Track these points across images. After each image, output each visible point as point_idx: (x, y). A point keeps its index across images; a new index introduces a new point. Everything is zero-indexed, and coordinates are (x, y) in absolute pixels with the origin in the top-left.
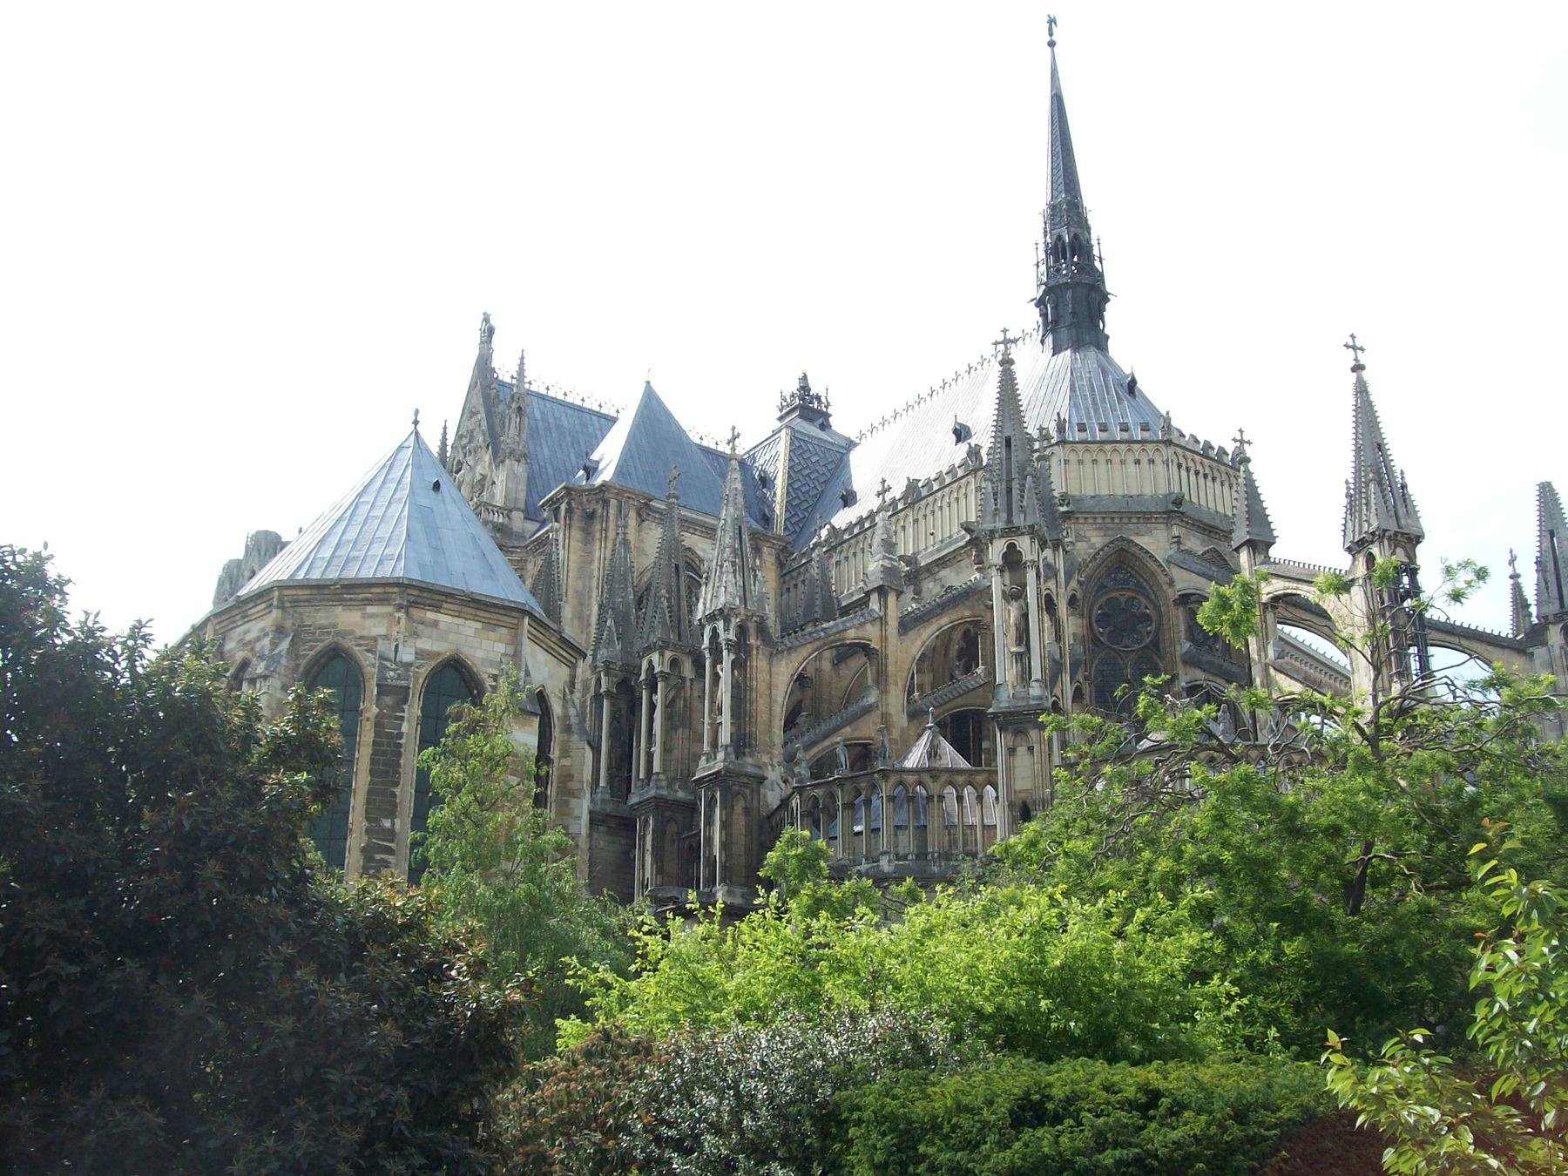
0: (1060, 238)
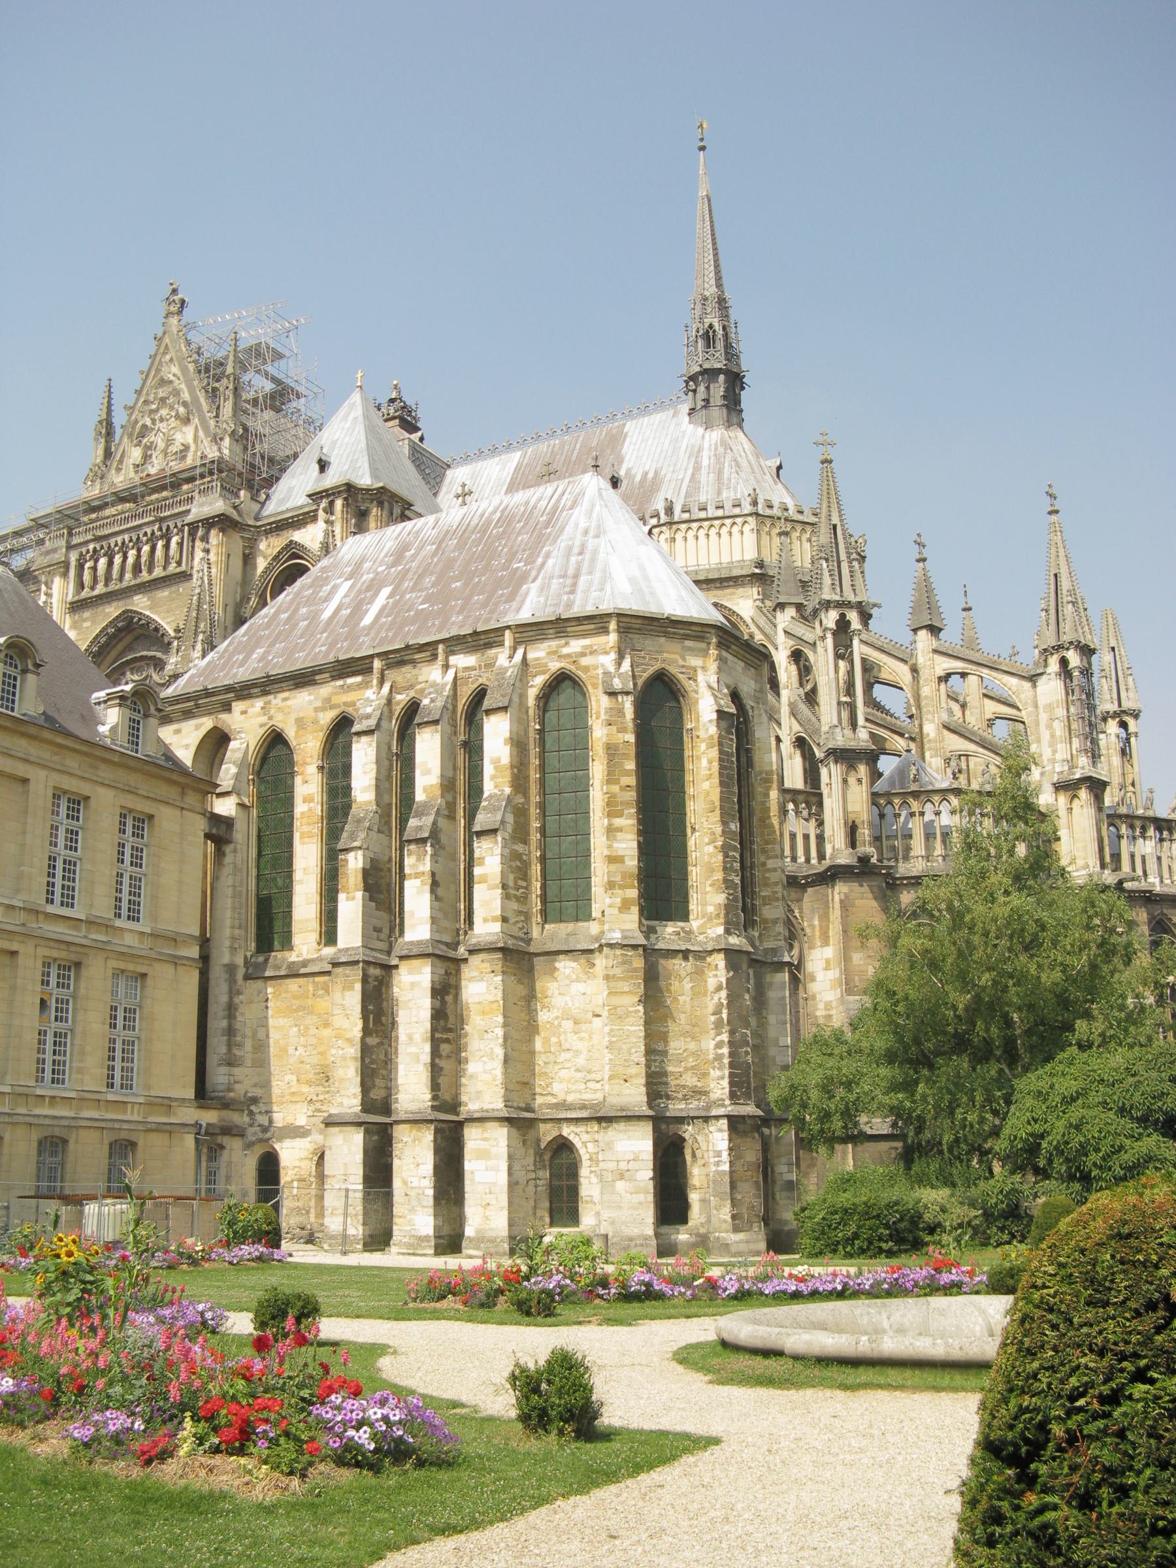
0: (711, 326)
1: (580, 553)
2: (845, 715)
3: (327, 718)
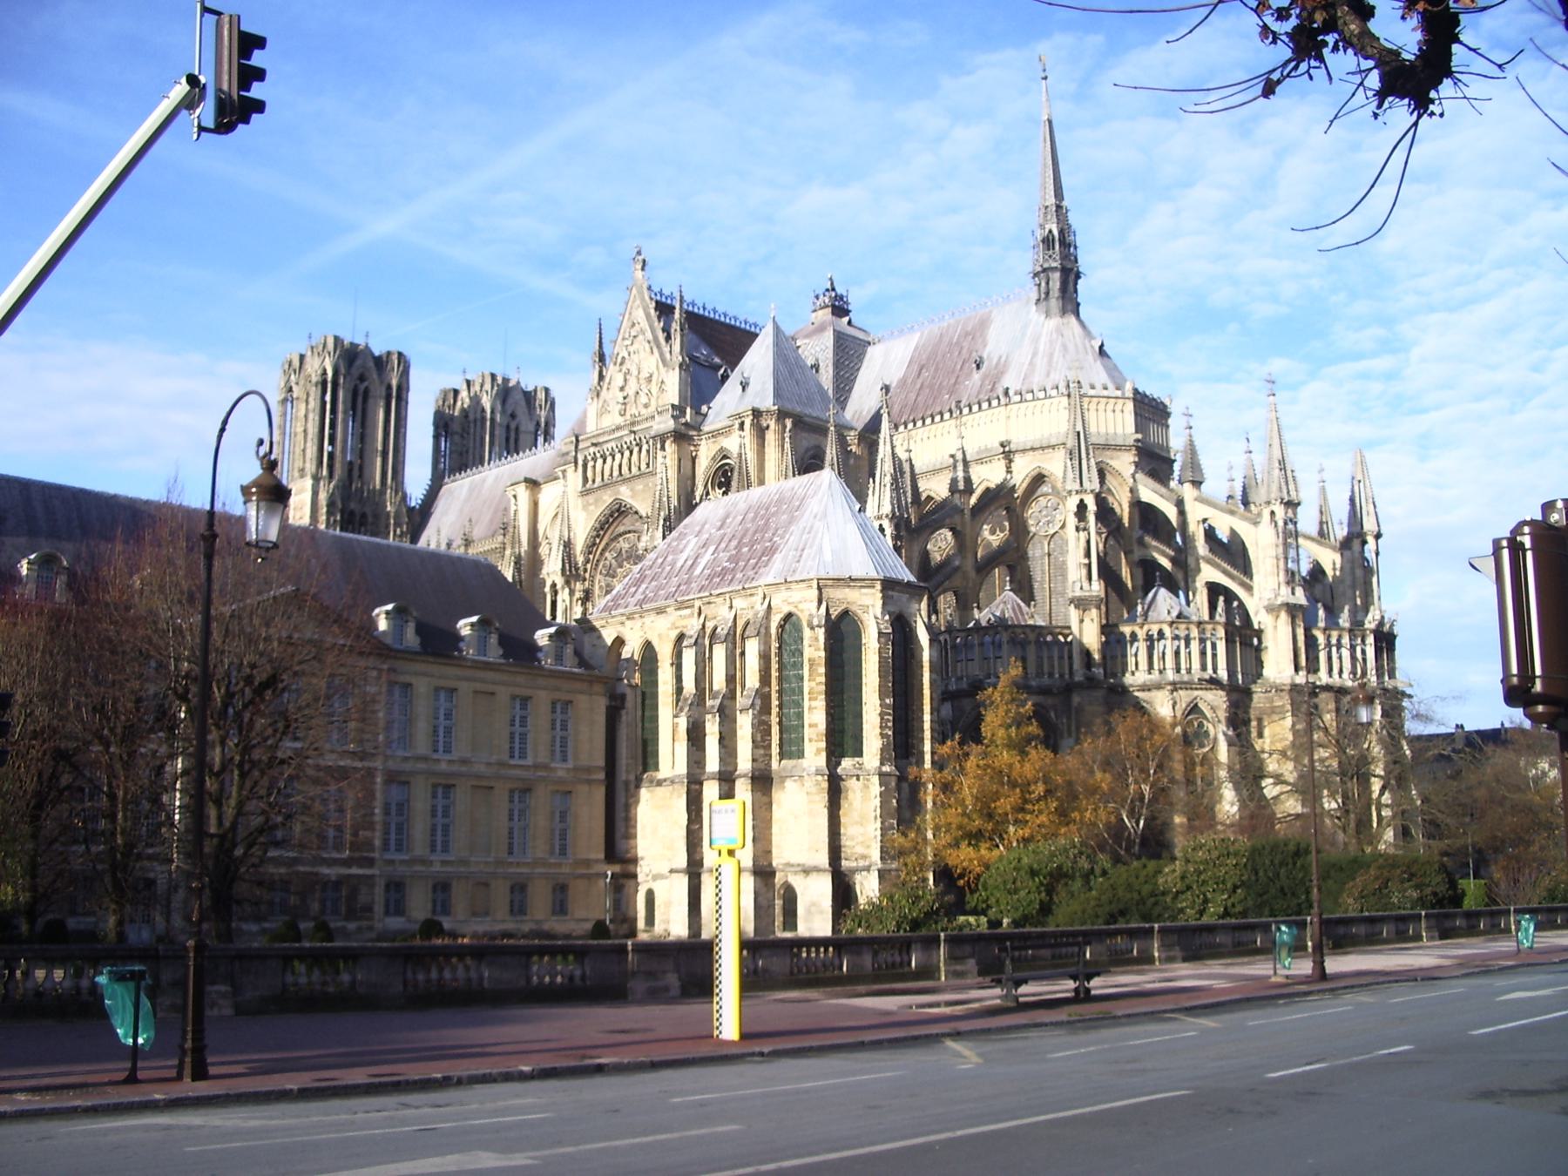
0: (1050, 231)
1: (809, 533)
2: (1084, 572)
3: (674, 634)
